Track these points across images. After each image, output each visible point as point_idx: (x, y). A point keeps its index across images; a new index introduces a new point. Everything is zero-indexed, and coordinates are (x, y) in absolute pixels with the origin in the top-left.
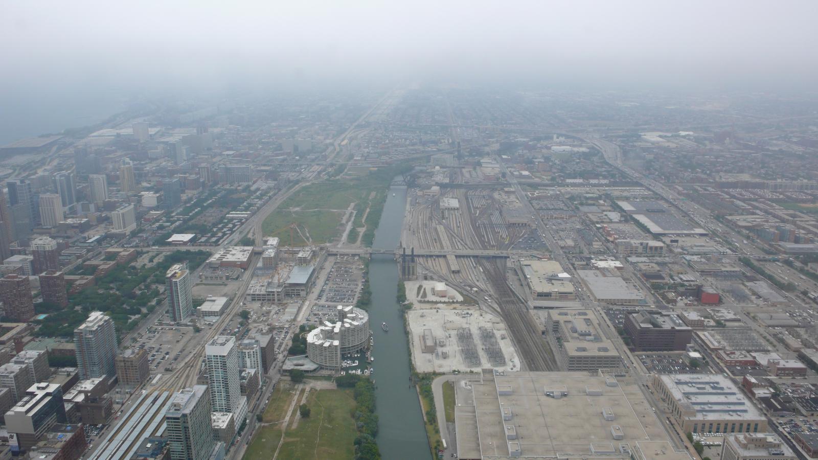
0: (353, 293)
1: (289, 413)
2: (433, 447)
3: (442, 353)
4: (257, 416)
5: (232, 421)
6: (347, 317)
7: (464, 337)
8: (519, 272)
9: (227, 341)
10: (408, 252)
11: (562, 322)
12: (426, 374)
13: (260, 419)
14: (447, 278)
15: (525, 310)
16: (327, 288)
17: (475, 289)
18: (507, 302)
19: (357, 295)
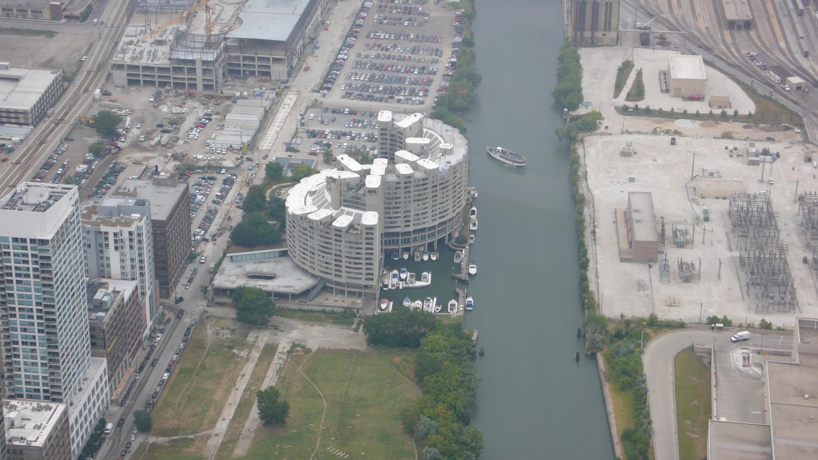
0: (424, 77)
1: (229, 412)
3: (681, 265)
4: (137, 414)
6: (403, 146)
9: (55, 197)
12: (628, 323)
13: (144, 425)
14: (711, 44)
16: (351, 57)
17: (795, 80)
19: (438, 82)
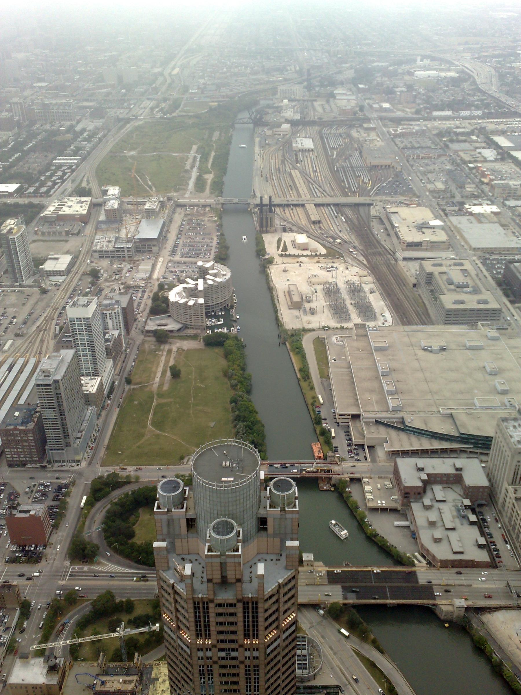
0: (209, 248)
1: (159, 375)
2: (310, 403)
3: (310, 309)
4: (126, 378)
5: (101, 385)
6: (208, 274)
7: (331, 292)
8: (386, 221)
10: (266, 201)
11: (436, 274)
12: (295, 330)
13: (129, 381)
14: (307, 230)
15: (393, 262)
16: (180, 242)
17: (338, 241)
18: (374, 254)
19: (214, 250)
